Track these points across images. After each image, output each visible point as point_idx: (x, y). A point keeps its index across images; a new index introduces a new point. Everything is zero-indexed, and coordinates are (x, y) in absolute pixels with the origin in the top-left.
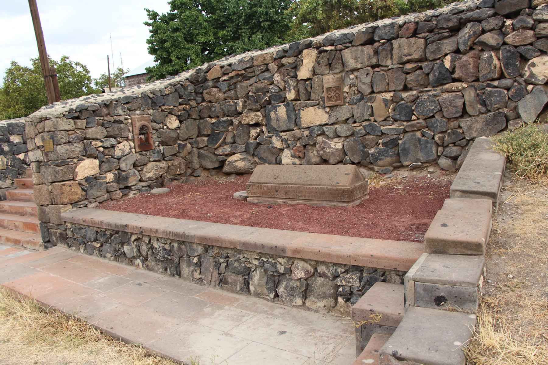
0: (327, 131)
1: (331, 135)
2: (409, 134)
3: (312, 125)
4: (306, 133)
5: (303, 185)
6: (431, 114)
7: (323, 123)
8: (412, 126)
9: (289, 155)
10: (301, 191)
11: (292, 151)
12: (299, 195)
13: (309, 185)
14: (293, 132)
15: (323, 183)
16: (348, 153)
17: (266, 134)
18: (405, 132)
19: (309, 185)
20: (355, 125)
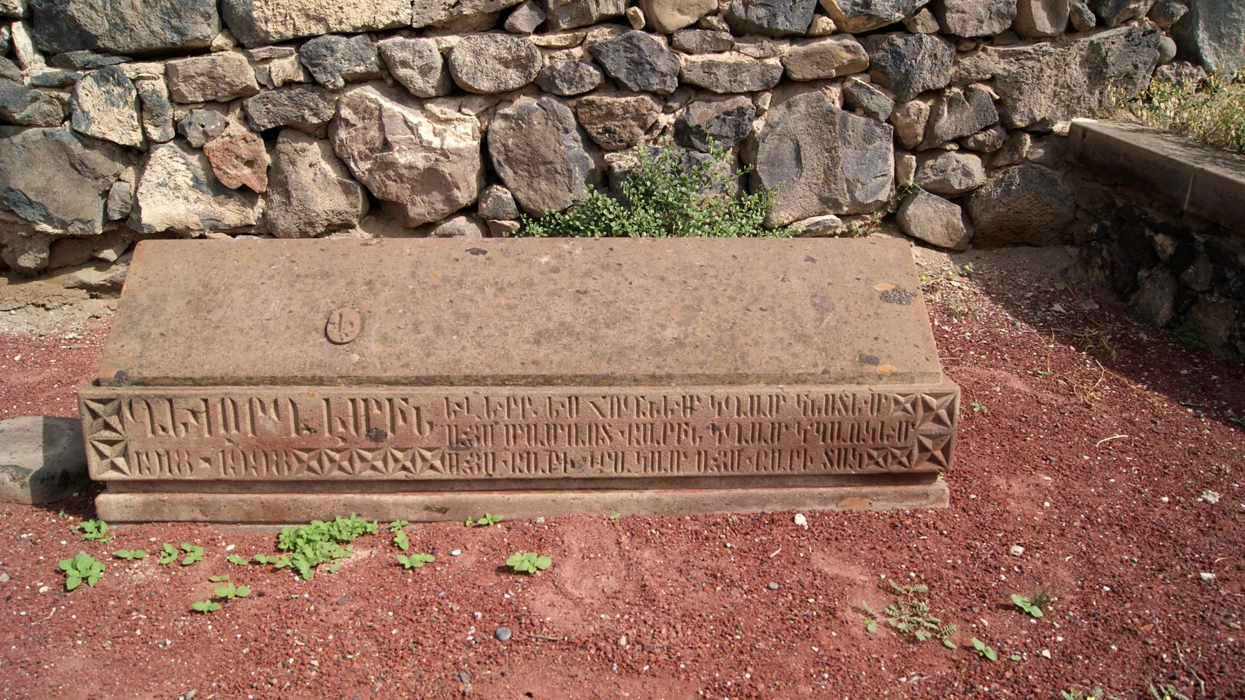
0: (404, 64)
1: (419, 83)
2: (802, 100)
3: (316, 29)
4: (285, 66)
5: (596, 381)
6: (898, 16)
7: (383, 21)
8: (823, 58)
9: (184, 178)
10: (593, 427)
11: (194, 159)
12: (574, 452)
13: (654, 379)
14: (203, 62)
15: (759, 359)
16: (507, 173)
17: (37, 67)
18: (786, 83)
19: (654, 379)
20: (552, 39)
